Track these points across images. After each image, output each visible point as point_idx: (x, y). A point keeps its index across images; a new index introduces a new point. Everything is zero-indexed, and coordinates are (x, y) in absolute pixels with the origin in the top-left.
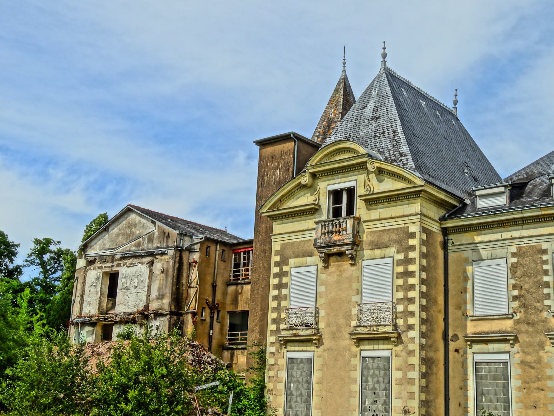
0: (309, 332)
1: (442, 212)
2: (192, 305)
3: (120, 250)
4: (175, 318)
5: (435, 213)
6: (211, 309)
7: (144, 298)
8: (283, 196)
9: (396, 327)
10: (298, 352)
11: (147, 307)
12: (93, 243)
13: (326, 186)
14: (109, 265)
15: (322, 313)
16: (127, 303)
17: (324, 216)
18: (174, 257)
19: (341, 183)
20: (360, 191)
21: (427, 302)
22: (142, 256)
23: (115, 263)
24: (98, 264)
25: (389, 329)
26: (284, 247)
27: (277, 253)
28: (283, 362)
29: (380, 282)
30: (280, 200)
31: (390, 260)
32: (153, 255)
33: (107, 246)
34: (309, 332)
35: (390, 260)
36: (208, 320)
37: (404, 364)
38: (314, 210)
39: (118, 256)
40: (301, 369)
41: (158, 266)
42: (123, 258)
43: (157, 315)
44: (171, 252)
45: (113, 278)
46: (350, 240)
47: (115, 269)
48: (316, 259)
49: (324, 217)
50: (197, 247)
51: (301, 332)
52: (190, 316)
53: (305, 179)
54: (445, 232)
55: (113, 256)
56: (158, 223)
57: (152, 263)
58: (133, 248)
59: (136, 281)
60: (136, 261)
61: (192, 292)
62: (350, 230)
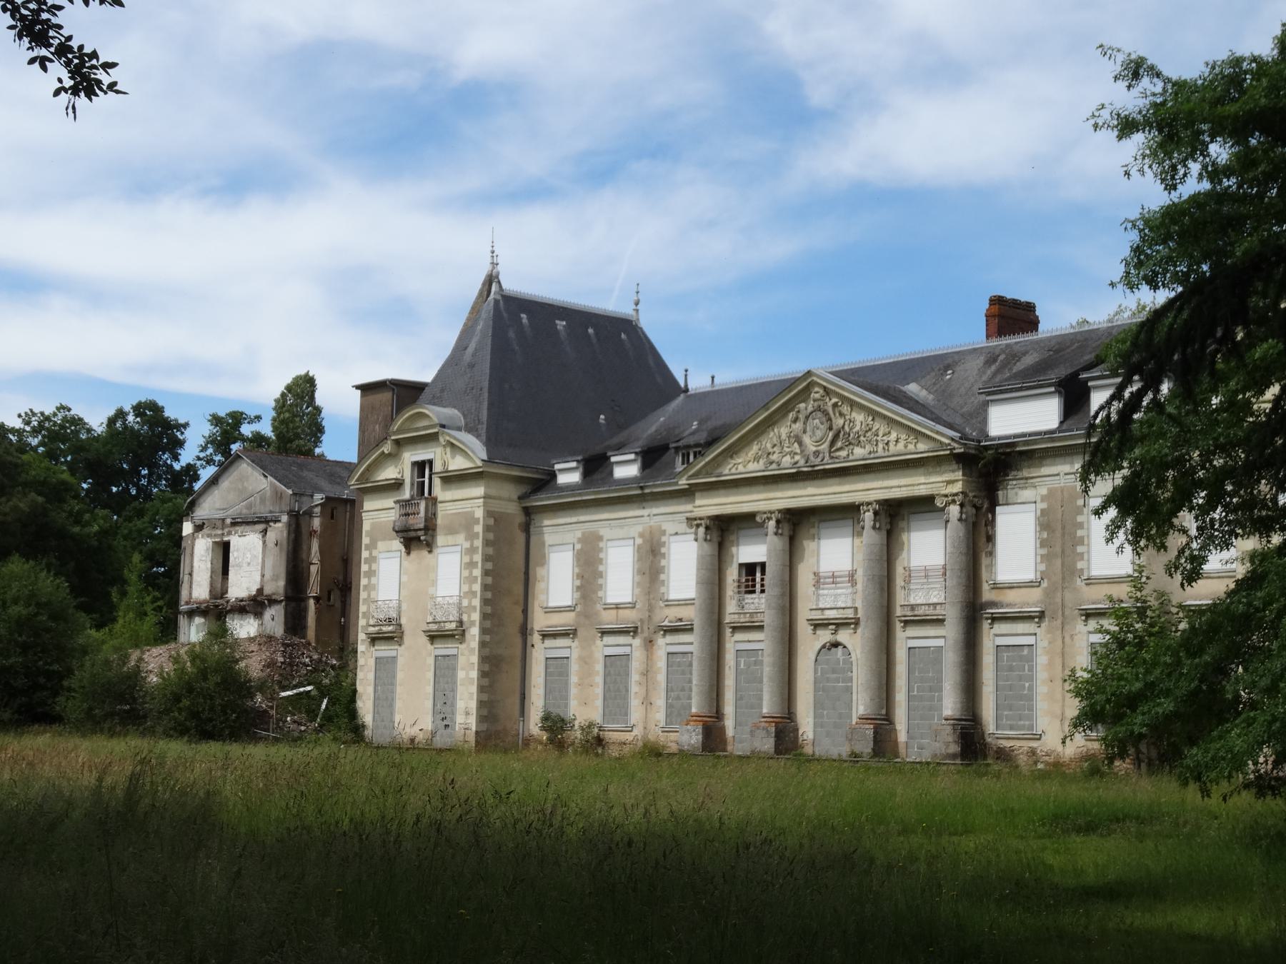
0: (390, 628)
1: (523, 489)
2: (314, 589)
3: (230, 512)
4: (293, 604)
5: (511, 491)
6: (341, 590)
7: (258, 578)
8: (369, 466)
9: (461, 623)
10: (384, 650)
11: (260, 591)
12: (201, 500)
13: (412, 456)
14: (220, 532)
15: (404, 607)
16: (241, 585)
17: (406, 494)
18: (289, 525)
19: (421, 454)
20: (438, 467)
21: (493, 594)
22: (254, 523)
23: (226, 530)
24: (205, 531)
25: (453, 626)
26: (373, 526)
27: (368, 534)
28: (372, 662)
29: (451, 576)
30: (367, 469)
31: (459, 548)
32: (267, 521)
33: (217, 506)
34: (390, 628)
35: (459, 548)
36: (338, 605)
37: (857, 643)
38: (397, 485)
39: (228, 521)
40: (385, 668)
41: (272, 535)
42: (234, 524)
43: (272, 602)
44: (285, 518)
45: (225, 548)
46: (422, 526)
47: (226, 539)
48: (397, 544)
49: (407, 495)
50: (318, 510)
51: (385, 629)
52: (312, 602)
53: (387, 448)
54: (528, 512)
55: (223, 520)
56: (270, 478)
57: (265, 532)
58: (245, 511)
59: (249, 555)
60: (248, 528)
61: (314, 569)
62: (422, 514)
